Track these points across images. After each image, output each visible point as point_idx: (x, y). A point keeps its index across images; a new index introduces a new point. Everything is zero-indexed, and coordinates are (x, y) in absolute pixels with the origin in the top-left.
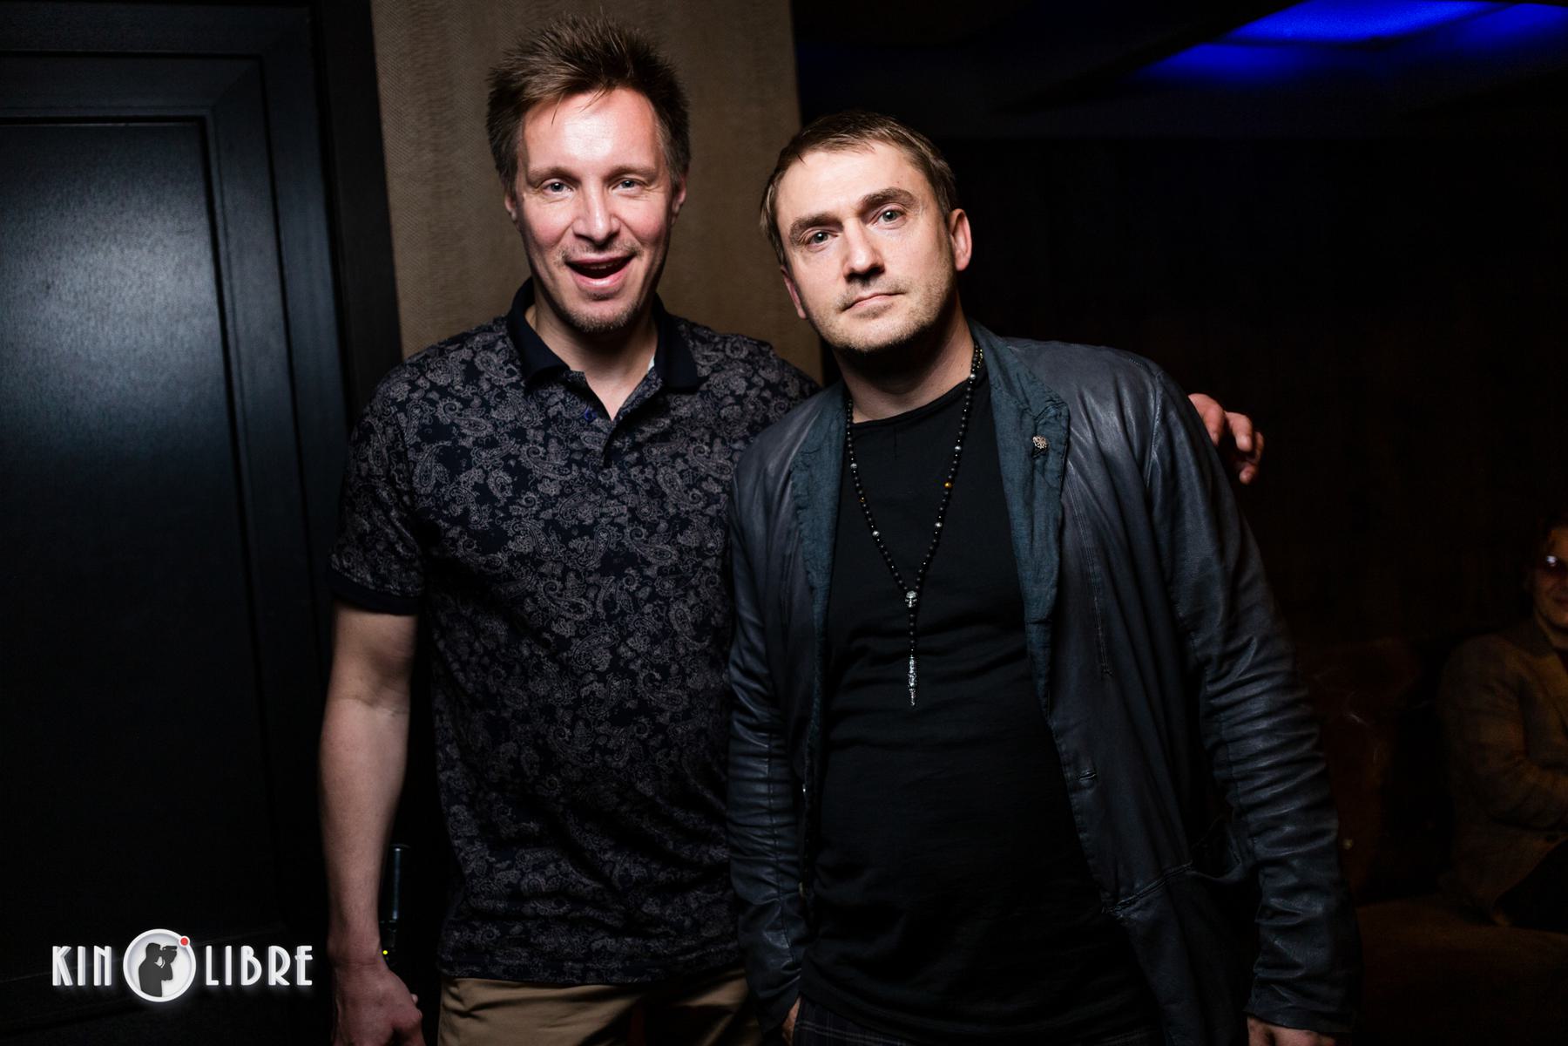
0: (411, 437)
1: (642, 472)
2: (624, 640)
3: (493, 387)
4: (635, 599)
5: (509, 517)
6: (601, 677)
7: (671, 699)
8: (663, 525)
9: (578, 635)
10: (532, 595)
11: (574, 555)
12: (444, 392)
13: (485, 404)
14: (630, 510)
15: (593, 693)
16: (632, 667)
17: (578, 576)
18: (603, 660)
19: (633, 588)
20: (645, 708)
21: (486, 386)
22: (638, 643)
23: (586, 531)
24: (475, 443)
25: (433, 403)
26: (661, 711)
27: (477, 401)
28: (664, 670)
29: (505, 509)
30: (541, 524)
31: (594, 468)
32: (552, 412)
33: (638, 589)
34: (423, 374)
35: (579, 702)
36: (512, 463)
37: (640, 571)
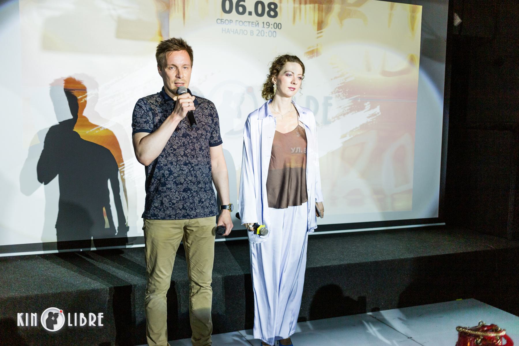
6: (182, 156)
18: (182, 153)
20: (190, 163)
22: (189, 151)
28: (193, 156)
35: (177, 161)
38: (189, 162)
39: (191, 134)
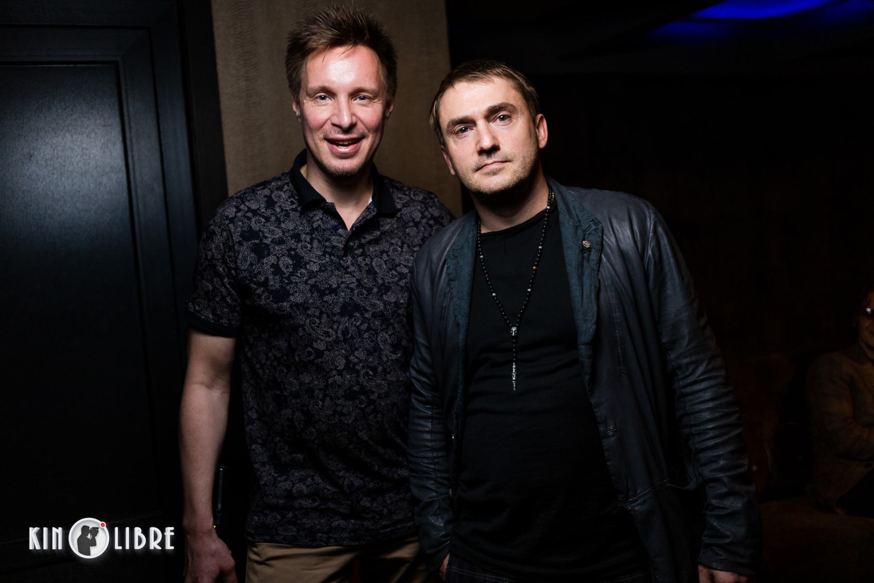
0: (236, 238)
1: (364, 260)
2: (353, 352)
3: (282, 210)
4: (359, 330)
5: (290, 282)
6: (340, 373)
7: (378, 386)
8: (375, 290)
9: (327, 349)
10: (303, 326)
11: (326, 305)
12: (255, 213)
13: (278, 220)
14: (357, 280)
15: (335, 381)
16: (357, 367)
17: (328, 316)
18: (341, 363)
19: (358, 324)
20: (364, 391)
21: (278, 210)
22: (360, 354)
23: (334, 291)
24: (272, 242)
25: (249, 219)
26: (373, 392)
27: (273, 218)
28: (374, 369)
29: (288, 278)
30: (308, 287)
31: (338, 257)
32: (315, 225)
33: (361, 324)
34: (243, 203)
36: (293, 253)
37: (362, 314)
38: (362, 387)
39: (367, 305)
